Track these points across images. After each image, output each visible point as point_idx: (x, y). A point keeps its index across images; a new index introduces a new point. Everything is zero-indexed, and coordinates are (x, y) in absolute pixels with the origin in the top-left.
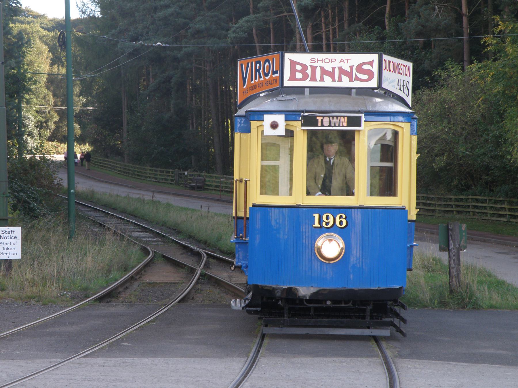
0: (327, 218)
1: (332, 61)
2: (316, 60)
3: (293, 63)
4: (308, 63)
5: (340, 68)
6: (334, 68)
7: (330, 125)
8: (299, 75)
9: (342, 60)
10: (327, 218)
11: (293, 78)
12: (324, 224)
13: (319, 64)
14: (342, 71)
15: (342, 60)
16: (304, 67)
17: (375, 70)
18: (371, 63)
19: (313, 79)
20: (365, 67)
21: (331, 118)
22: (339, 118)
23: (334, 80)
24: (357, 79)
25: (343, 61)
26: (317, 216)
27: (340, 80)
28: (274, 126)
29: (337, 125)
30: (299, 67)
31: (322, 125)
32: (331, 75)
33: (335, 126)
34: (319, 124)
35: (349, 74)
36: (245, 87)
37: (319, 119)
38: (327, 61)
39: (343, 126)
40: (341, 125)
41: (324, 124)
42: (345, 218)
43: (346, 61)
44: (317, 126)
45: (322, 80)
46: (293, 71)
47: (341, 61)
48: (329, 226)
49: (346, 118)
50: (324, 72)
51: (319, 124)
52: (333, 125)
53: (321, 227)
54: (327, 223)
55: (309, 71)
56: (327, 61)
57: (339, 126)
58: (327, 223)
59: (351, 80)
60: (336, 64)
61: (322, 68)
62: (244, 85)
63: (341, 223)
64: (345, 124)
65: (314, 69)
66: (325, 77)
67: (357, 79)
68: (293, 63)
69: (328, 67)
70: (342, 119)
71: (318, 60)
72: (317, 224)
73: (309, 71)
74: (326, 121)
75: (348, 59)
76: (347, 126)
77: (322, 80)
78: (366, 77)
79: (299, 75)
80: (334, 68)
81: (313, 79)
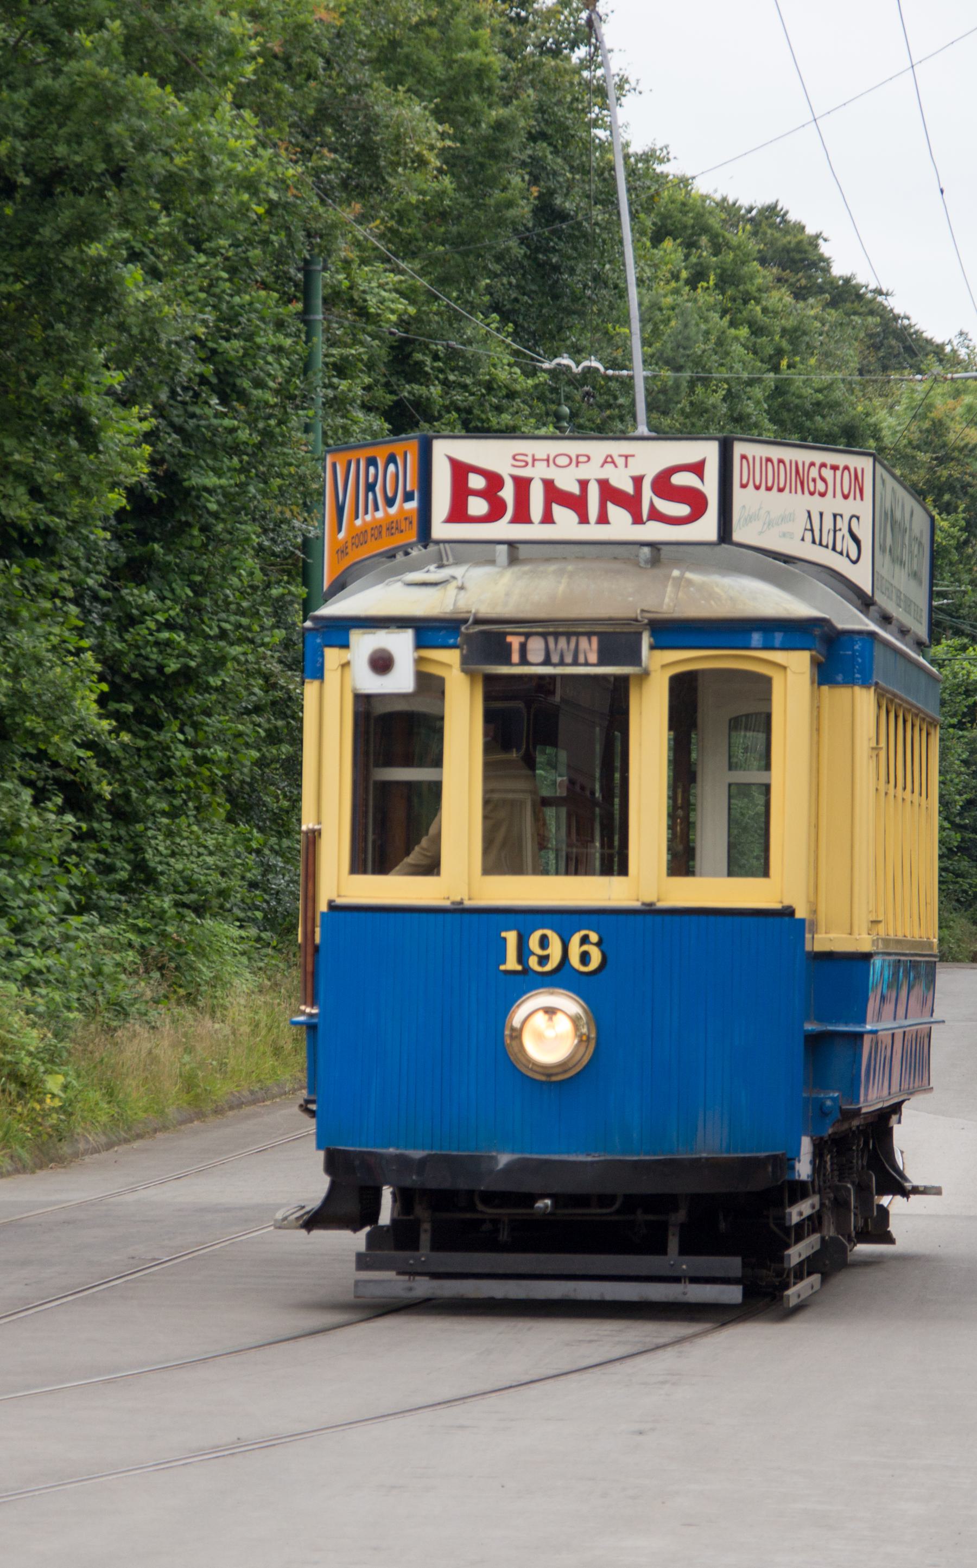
0: (544, 942)
1: (578, 463)
2: (529, 460)
3: (460, 471)
4: (505, 470)
5: (604, 485)
6: (584, 484)
7: (547, 662)
8: (477, 506)
9: (609, 460)
10: (544, 942)
11: (458, 514)
12: (533, 962)
13: (537, 473)
14: (609, 493)
15: (609, 460)
16: (494, 481)
17: (710, 487)
18: (698, 469)
19: (522, 516)
20: (679, 479)
21: (551, 640)
22: (573, 640)
23: (584, 519)
24: (656, 515)
25: (613, 462)
26: (511, 937)
27: (603, 519)
28: (382, 663)
29: (569, 659)
30: (477, 482)
31: (524, 661)
32: (577, 504)
33: (562, 663)
34: (515, 658)
35: (631, 503)
36: (341, 536)
37: (515, 642)
38: (563, 461)
39: (587, 664)
40: (581, 659)
41: (531, 658)
42: (598, 944)
43: (620, 462)
44: (507, 661)
45: (548, 518)
46: (460, 493)
47: (605, 462)
48: (549, 967)
49: (595, 640)
50: (553, 494)
51: (515, 658)
52: (555, 659)
53: (526, 970)
54: (543, 960)
55: (508, 493)
56: (563, 461)
57: (575, 663)
58: (543, 960)
59: (637, 519)
60: (593, 472)
61: (549, 485)
62: (340, 530)
63: (585, 958)
64: (593, 658)
65: (522, 485)
66: (558, 511)
67: (656, 515)
68: (460, 471)
69: (567, 483)
70: (584, 642)
71: (534, 460)
72: (512, 963)
73: (508, 493)
74: (536, 648)
75: (626, 457)
76: (601, 663)
77: (548, 518)
78: (682, 510)
79: (477, 506)
80: (584, 484)
81: (522, 516)
